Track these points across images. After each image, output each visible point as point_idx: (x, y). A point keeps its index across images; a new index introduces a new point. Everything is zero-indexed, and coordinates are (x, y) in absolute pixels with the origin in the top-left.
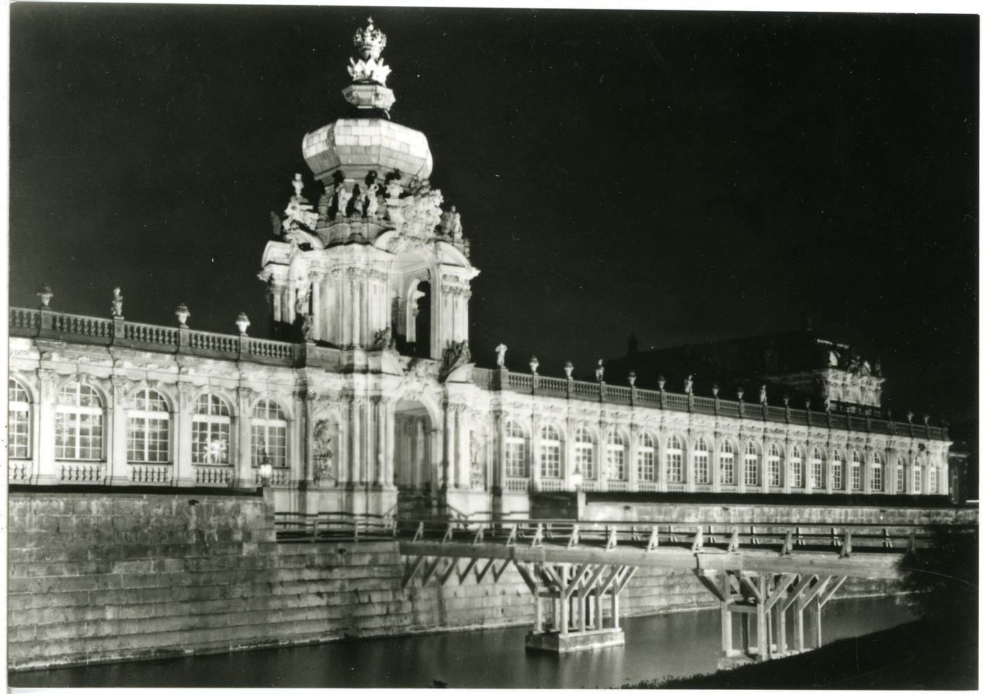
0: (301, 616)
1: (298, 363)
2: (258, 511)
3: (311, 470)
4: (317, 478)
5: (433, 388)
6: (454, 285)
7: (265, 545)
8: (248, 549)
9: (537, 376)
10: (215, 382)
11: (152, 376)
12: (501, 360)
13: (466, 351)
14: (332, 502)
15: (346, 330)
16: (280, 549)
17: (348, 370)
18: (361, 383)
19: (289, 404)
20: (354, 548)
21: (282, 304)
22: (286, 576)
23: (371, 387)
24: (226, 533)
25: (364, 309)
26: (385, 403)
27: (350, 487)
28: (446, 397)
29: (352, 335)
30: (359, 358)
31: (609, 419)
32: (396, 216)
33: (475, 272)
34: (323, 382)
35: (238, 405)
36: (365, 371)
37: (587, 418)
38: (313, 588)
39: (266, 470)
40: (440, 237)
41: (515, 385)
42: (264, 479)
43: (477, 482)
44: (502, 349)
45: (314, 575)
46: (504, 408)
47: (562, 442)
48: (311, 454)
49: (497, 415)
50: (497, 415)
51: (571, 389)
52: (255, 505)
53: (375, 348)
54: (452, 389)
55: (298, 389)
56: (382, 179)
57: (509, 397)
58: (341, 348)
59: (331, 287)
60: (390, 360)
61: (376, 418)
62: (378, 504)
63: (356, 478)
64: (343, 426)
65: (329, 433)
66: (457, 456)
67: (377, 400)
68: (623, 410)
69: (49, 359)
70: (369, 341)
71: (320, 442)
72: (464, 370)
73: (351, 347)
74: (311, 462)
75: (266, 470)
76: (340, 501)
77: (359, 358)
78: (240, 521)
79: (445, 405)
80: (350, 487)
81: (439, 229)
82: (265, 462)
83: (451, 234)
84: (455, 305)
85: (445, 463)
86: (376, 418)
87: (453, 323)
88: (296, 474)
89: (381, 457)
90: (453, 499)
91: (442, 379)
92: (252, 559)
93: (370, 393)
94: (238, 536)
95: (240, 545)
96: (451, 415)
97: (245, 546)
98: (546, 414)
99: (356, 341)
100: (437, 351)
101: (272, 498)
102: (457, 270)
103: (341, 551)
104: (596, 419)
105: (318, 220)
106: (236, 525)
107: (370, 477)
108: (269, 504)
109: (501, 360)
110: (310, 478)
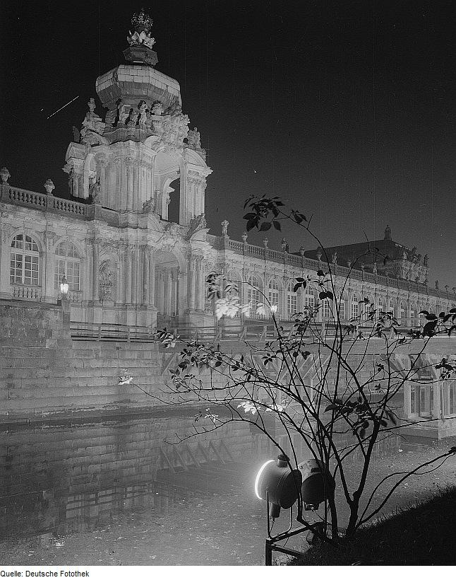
2: (58, 318)
3: (97, 291)
4: (101, 300)
5: (181, 244)
6: (196, 178)
7: (61, 341)
8: (49, 344)
9: (246, 244)
12: (225, 230)
13: (203, 220)
14: (111, 317)
15: (124, 200)
16: (75, 345)
17: (126, 226)
18: (132, 234)
19: (82, 247)
20: (127, 347)
21: (80, 185)
22: (75, 363)
23: (140, 238)
24: (34, 331)
25: (137, 186)
26: (150, 250)
27: (125, 306)
29: (128, 203)
30: (132, 219)
31: (289, 276)
33: (210, 172)
34: (106, 232)
37: (276, 274)
38: (98, 374)
39: (64, 288)
41: (233, 248)
42: (64, 295)
43: (208, 310)
44: (226, 223)
46: (227, 262)
47: (261, 287)
48: (97, 283)
50: (222, 265)
51: (267, 255)
52: (56, 312)
54: (193, 246)
55: (88, 236)
60: (152, 221)
61: (144, 261)
62: (144, 319)
63: (129, 301)
64: (120, 265)
65: (110, 269)
66: (197, 291)
67: (144, 248)
71: (104, 275)
72: (202, 233)
73: (127, 211)
74: (97, 286)
75: (64, 288)
76: (117, 317)
78: (44, 323)
79: (189, 256)
80: (125, 306)
82: (64, 281)
85: (189, 295)
86: (144, 261)
87: (194, 203)
88: (87, 296)
89: (146, 287)
90: (194, 319)
92: (52, 351)
94: (42, 334)
95: (43, 340)
97: (48, 340)
98: (252, 269)
100: (185, 218)
101: (67, 307)
102: (197, 168)
103: (118, 348)
106: (41, 325)
107: (138, 300)
108: (66, 311)
109: (225, 230)
110: (97, 298)
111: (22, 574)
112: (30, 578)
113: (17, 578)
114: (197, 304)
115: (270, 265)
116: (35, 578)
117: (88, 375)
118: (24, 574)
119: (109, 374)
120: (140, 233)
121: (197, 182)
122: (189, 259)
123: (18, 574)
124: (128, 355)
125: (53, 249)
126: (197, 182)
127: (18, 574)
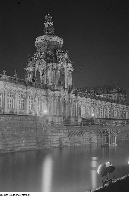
5: (67, 95)
6: (70, 72)
18: (56, 92)
23: (58, 94)
33: (73, 70)
36: (57, 91)
54: (71, 95)
62: (61, 119)
67: (60, 97)
77: (56, 88)
84: (70, 77)
87: (69, 81)
89: (61, 109)
93: (58, 96)
111: (7, 195)
112: (10, 196)
113: (6, 196)
116: (12, 196)
117: (53, 137)
118: (8, 195)
120: (59, 92)
121: (70, 74)
122: (69, 100)
123: (6, 195)
126: (70, 74)
127: (6, 195)
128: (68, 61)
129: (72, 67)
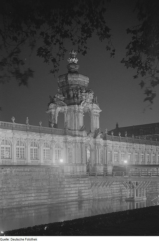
0: (71, 196)
1: (65, 134)
5: (93, 140)
9: (113, 136)
10: (47, 139)
11: (35, 138)
17: (75, 136)
18: (78, 138)
28: (96, 142)
30: (77, 133)
31: (129, 147)
32: (84, 97)
33: (101, 111)
35: (52, 145)
38: (73, 189)
40: (93, 102)
45: (73, 186)
49: (105, 145)
50: (105, 145)
53: (81, 130)
54: (97, 140)
56: (79, 88)
57: (108, 141)
58: (72, 130)
59: (69, 115)
67: (82, 143)
68: (131, 144)
69: (15, 135)
70: (80, 128)
77: (77, 133)
79: (95, 144)
81: (93, 100)
83: (95, 101)
84: (97, 119)
85: (96, 158)
87: (96, 124)
89: (83, 157)
91: (95, 137)
93: (80, 141)
96: (97, 146)
99: (76, 128)
104: (126, 147)
105: (65, 98)
114: (99, 162)
115: (122, 143)
119: (76, 189)
120: (80, 138)
121: (97, 116)
122: (95, 145)
124: (81, 182)
125: (54, 146)
126: (97, 116)
128: (93, 101)
129: (99, 108)
